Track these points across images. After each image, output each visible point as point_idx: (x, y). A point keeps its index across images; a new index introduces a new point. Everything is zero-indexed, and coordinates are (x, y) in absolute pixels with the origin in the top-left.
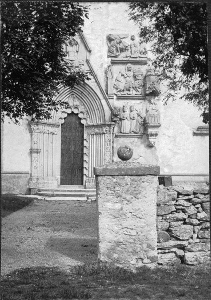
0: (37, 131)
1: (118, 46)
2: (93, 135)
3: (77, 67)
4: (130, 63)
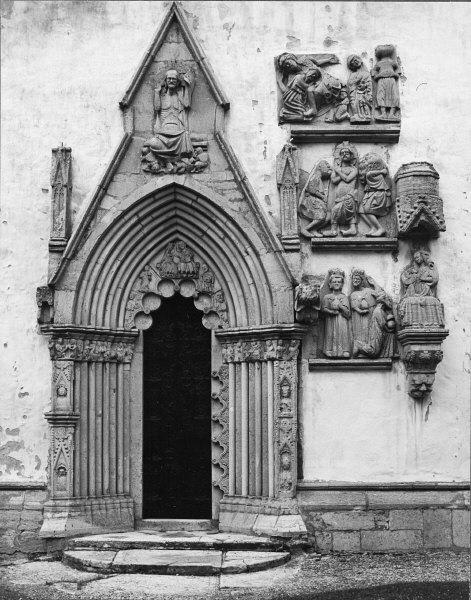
0: (68, 357)
1: (311, 89)
2: (240, 363)
3: (188, 155)
4: (346, 139)
